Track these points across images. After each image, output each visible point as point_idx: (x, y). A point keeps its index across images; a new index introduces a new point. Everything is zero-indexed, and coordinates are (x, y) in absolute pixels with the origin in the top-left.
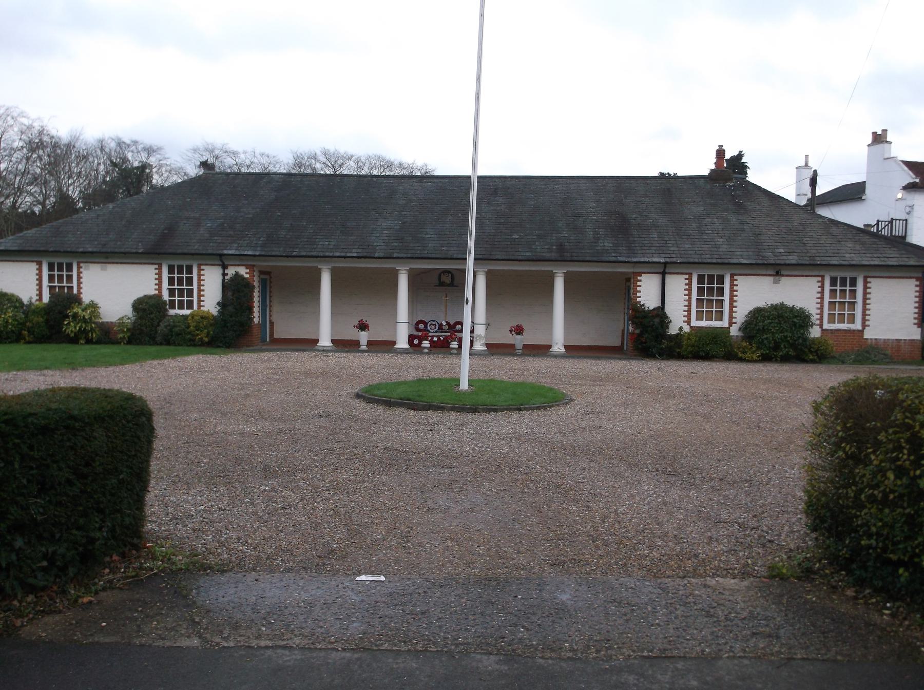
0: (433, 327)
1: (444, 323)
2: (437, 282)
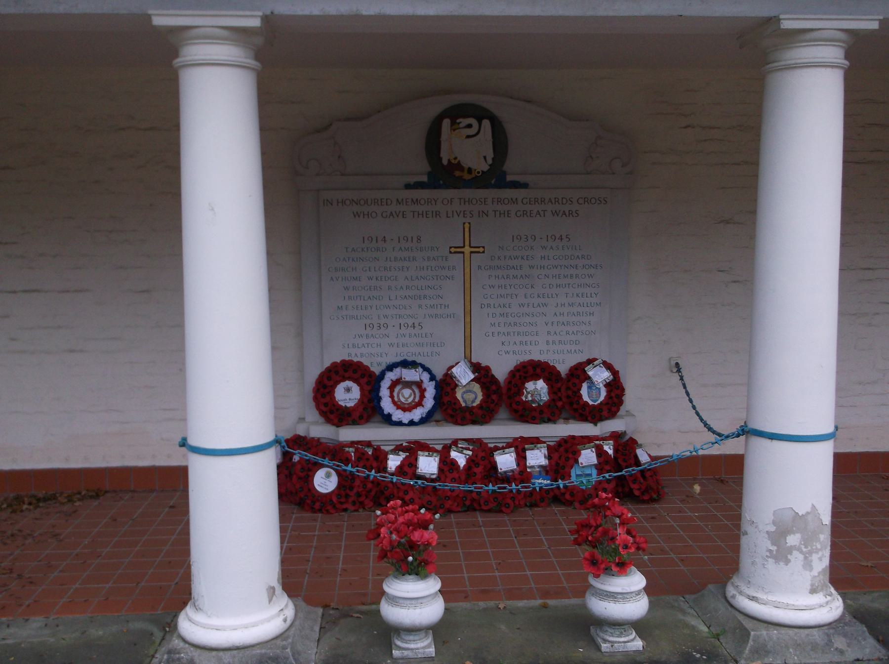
0: (406, 395)
1: (464, 375)
2: (420, 168)
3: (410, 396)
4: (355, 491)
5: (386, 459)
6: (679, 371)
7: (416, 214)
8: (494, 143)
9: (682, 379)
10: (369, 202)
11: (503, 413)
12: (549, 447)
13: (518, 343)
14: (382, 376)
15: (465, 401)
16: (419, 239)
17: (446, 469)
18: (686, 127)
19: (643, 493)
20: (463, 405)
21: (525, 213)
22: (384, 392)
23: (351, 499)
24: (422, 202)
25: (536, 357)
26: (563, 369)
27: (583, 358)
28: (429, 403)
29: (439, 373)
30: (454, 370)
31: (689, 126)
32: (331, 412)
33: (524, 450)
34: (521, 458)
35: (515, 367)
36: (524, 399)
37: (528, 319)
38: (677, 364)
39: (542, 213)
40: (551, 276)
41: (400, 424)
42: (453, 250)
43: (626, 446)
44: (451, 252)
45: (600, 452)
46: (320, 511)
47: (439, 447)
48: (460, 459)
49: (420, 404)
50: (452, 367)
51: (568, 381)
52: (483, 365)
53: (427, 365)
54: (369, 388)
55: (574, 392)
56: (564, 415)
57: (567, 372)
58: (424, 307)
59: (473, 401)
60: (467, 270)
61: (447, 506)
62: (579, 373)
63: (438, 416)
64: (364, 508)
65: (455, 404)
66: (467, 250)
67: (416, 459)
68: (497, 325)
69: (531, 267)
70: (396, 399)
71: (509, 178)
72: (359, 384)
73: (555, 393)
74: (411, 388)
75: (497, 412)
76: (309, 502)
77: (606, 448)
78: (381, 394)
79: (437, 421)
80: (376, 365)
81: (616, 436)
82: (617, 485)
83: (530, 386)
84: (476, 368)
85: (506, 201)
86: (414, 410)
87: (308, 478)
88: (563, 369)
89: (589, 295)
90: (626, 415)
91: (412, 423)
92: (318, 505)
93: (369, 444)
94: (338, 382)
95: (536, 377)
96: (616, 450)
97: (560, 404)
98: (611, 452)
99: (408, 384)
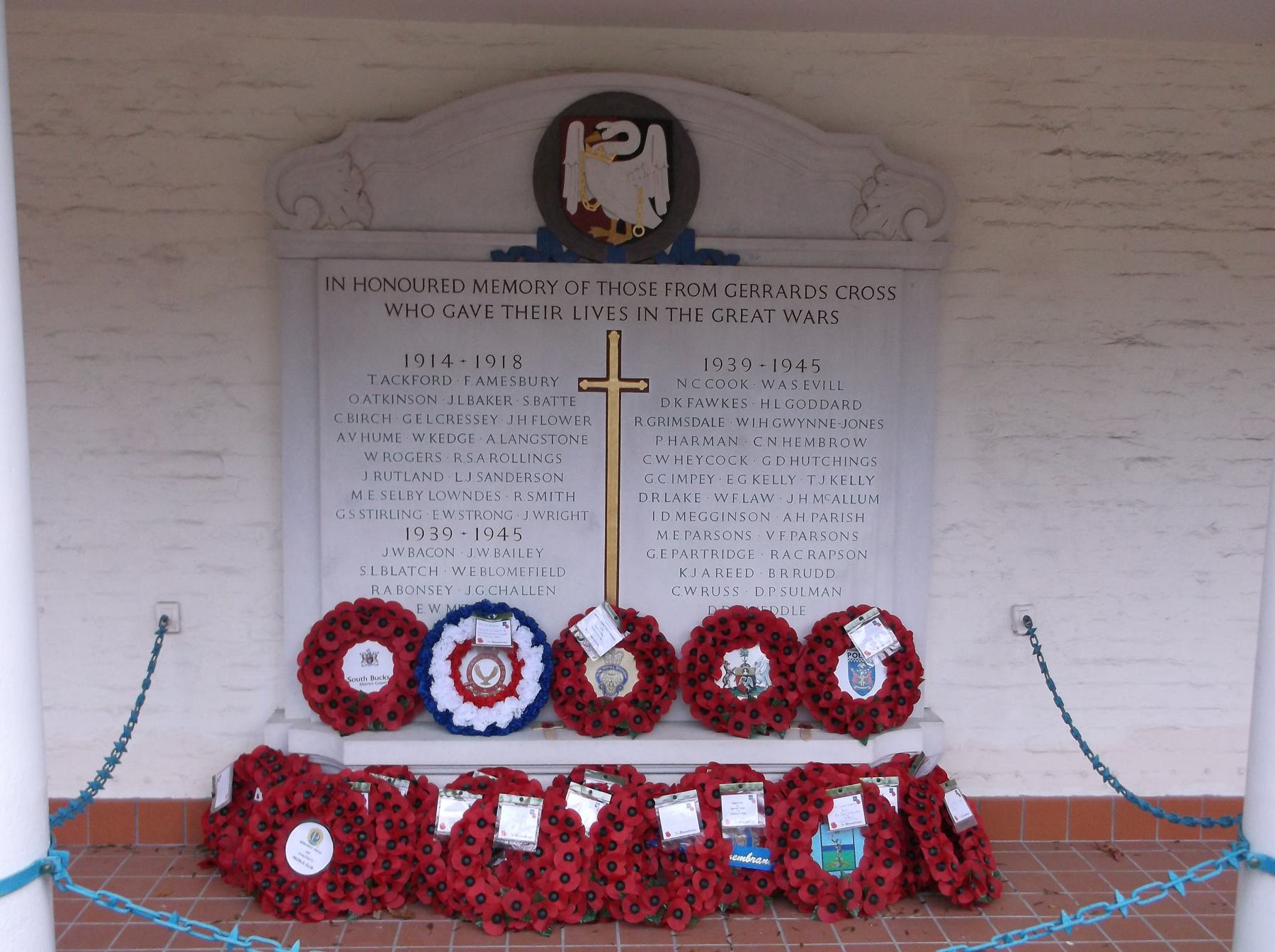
0: (486, 672)
1: (600, 634)
2: (525, 222)
3: (493, 675)
4: (367, 873)
5: (434, 805)
6: (1031, 633)
7: (512, 311)
8: (670, 171)
9: (1037, 651)
10: (419, 285)
11: (679, 711)
12: (769, 790)
13: (712, 573)
14: (439, 628)
15: (603, 687)
16: (517, 361)
17: (555, 833)
18: (1053, 153)
19: (957, 892)
20: (600, 694)
21: (730, 314)
22: (440, 667)
23: (356, 893)
24: (526, 287)
25: (747, 601)
26: (802, 625)
27: (841, 606)
28: (529, 689)
29: (553, 633)
30: (581, 624)
31: (1060, 151)
32: (333, 704)
33: (717, 794)
34: (710, 811)
35: (706, 620)
36: (720, 684)
37: (732, 526)
38: (1027, 620)
39: (765, 315)
40: (780, 442)
41: (469, 731)
42: (585, 384)
43: (924, 785)
44: (580, 389)
45: (872, 801)
46: (292, 914)
47: (546, 782)
48: (586, 807)
49: (511, 691)
50: (578, 618)
51: (812, 651)
52: (642, 614)
53: (529, 612)
54: (410, 656)
55: (821, 674)
56: (801, 716)
57: (809, 632)
58: (524, 496)
59: (619, 688)
60: (613, 426)
61: (553, 914)
62: (832, 635)
63: (549, 714)
64: (384, 908)
65: (582, 692)
66: (614, 384)
67: (495, 810)
68: (670, 535)
69: (742, 422)
70: (464, 680)
71: (700, 244)
72: (391, 648)
73: (783, 674)
74: (495, 658)
75: (666, 710)
76: (271, 894)
77: (884, 791)
78: (432, 671)
79: (547, 725)
80: (426, 609)
81: (903, 765)
82: (905, 870)
83: (733, 659)
84: (627, 619)
85: (694, 290)
86: (499, 705)
87: (274, 843)
88: (802, 625)
89: (855, 481)
90: (925, 720)
91: (493, 731)
92: (289, 901)
93: (403, 772)
94: (351, 644)
95: (744, 642)
96: (904, 796)
97: (792, 696)
98: (893, 801)
99: (490, 652)
